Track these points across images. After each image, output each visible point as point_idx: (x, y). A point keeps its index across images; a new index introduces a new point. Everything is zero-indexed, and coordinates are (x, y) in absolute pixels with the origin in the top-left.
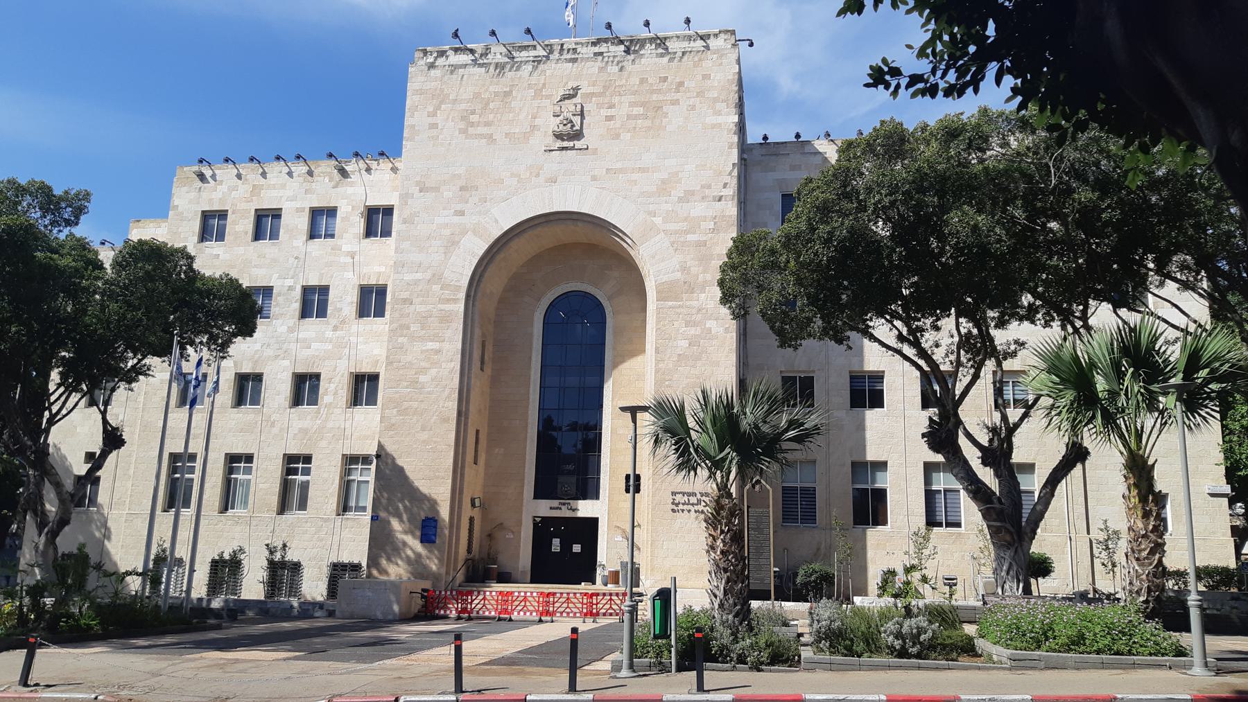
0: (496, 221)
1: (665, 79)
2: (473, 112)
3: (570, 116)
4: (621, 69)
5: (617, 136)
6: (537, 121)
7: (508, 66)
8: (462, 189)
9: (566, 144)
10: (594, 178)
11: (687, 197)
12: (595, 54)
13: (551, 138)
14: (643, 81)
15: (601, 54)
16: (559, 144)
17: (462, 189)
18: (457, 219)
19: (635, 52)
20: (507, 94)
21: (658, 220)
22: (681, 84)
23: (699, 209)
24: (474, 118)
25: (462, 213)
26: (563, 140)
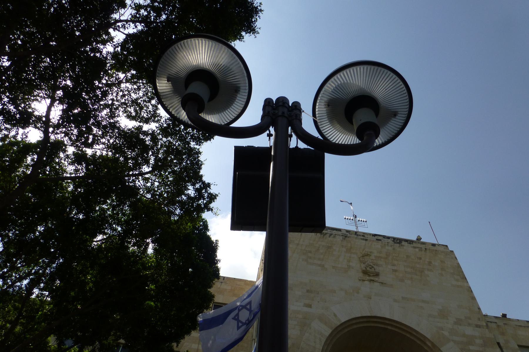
0: (335, 315)
1: (420, 259)
2: (310, 252)
3: (372, 264)
4: (394, 249)
5: (402, 280)
6: (351, 264)
7: (328, 235)
8: (308, 291)
9: (372, 278)
10: (395, 301)
11: (458, 322)
12: (377, 240)
13: (361, 275)
14: (408, 257)
15: (380, 240)
16: (368, 278)
17: (308, 291)
18: (306, 309)
19: (398, 243)
20: (329, 247)
21: (446, 333)
22: (430, 263)
23: (469, 331)
24: (310, 255)
25: (310, 306)
26: (369, 276)
